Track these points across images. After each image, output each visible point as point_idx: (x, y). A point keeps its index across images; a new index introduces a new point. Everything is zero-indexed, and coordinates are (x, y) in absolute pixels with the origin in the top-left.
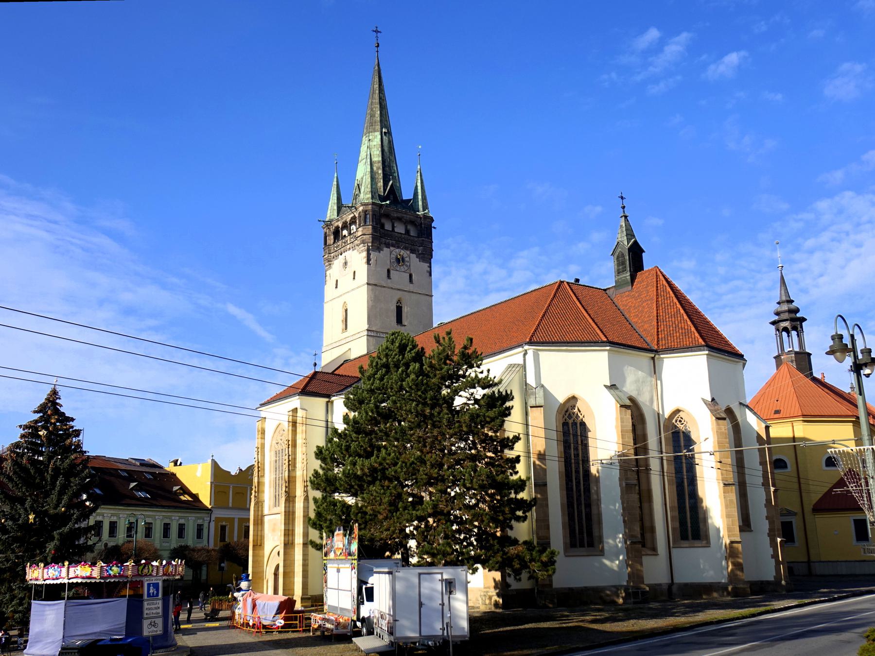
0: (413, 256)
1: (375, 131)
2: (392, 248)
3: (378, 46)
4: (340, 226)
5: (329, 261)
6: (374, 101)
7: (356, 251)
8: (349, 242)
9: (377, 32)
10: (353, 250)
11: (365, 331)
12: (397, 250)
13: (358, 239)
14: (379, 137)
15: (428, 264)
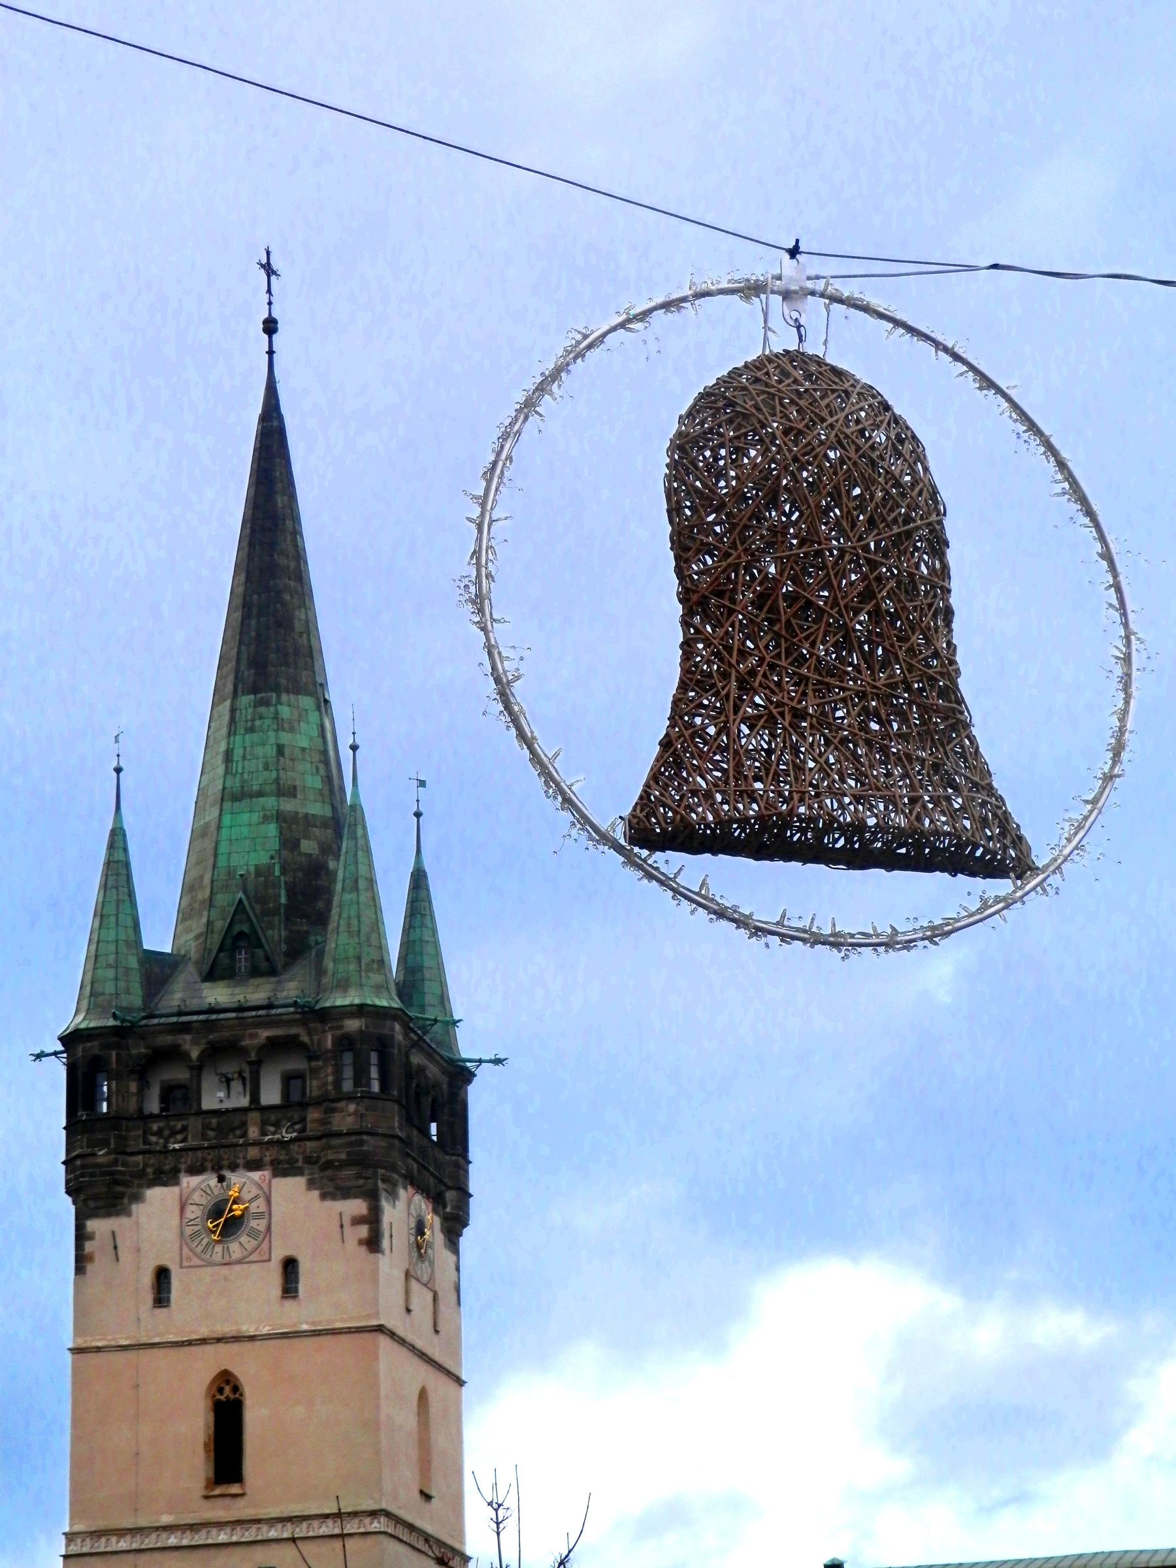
0: (437, 1221)
1: (297, 693)
2: (410, 1190)
3: (270, 326)
4: (195, 1054)
5: (117, 1183)
6: (282, 561)
7: (299, 1182)
8: (253, 1132)
9: (269, 270)
10: (285, 1173)
11: (373, 1514)
12: (418, 1198)
13: (336, 1141)
14: (314, 717)
15: (453, 1258)
